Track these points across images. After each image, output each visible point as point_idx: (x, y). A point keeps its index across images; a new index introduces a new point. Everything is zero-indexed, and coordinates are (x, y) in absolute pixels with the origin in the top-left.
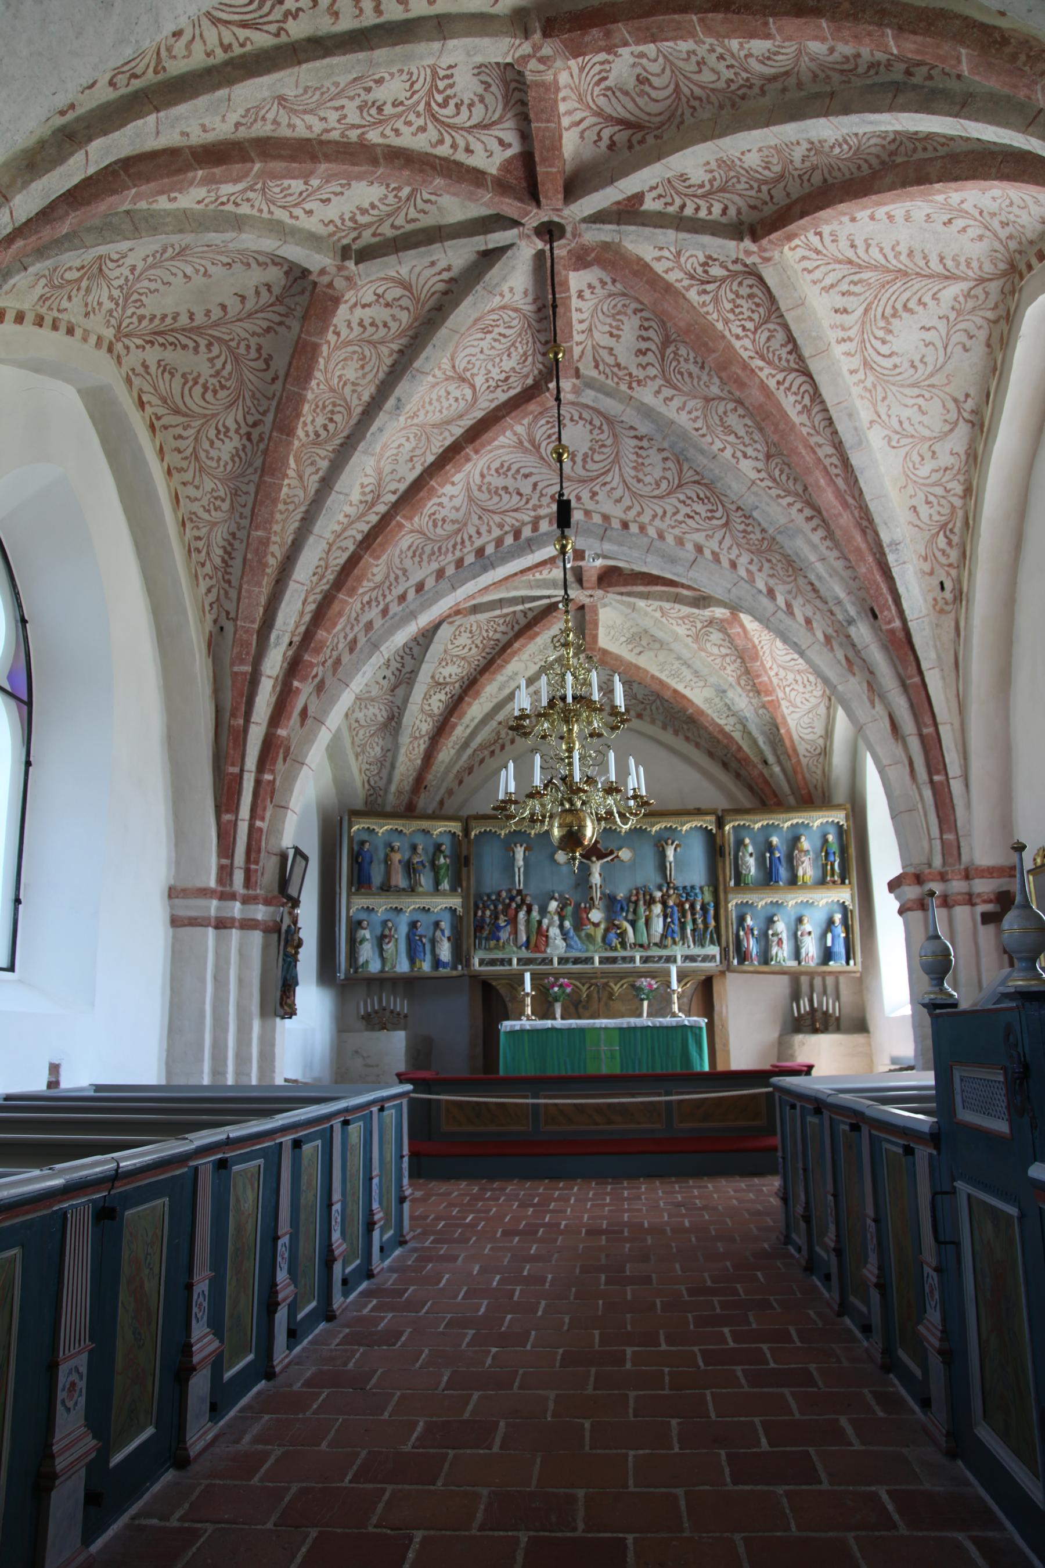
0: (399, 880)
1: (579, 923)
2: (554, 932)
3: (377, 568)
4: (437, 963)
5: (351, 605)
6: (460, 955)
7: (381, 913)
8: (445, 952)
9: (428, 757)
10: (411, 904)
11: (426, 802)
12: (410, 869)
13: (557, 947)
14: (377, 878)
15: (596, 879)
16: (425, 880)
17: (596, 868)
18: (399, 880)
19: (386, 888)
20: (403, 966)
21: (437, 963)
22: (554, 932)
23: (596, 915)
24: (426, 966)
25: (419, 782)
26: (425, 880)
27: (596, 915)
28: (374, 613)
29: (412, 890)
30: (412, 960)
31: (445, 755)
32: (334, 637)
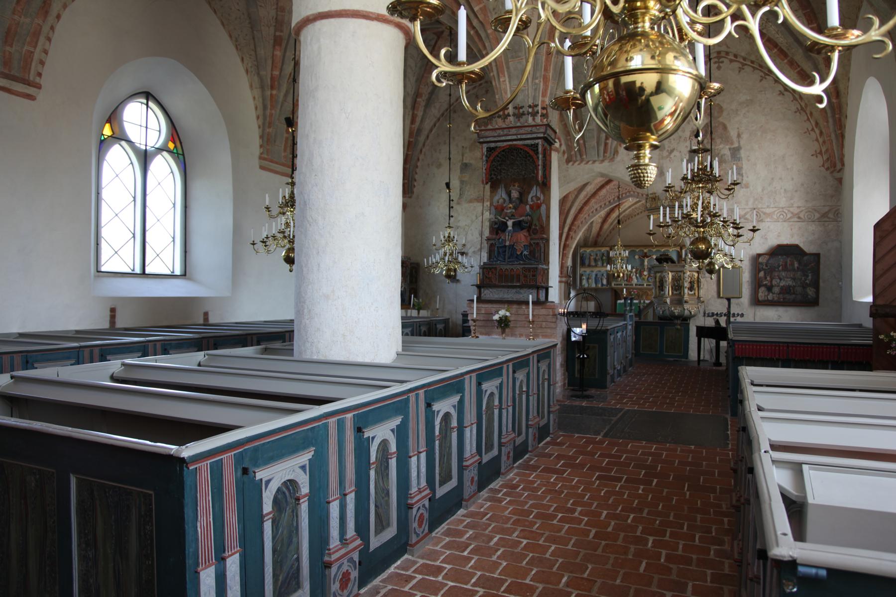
0: (593, 263)
1: (641, 275)
2: (634, 277)
3: (586, 208)
4: (602, 285)
5: (581, 216)
6: (609, 283)
7: (588, 272)
8: (605, 282)
9: (601, 228)
10: (596, 270)
11: (601, 240)
12: (595, 260)
13: (635, 281)
14: (587, 262)
15: (646, 263)
16: (600, 263)
17: (646, 260)
18: (593, 263)
19: (589, 266)
20: (594, 286)
21: (602, 285)
22: (634, 277)
23: (645, 273)
24: (600, 286)
25: (598, 235)
26: (600, 263)
27: (645, 273)
28: (586, 216)
29: (596, 266)
30: (596, 283)
31: (606, 226)
32: (577, 223)
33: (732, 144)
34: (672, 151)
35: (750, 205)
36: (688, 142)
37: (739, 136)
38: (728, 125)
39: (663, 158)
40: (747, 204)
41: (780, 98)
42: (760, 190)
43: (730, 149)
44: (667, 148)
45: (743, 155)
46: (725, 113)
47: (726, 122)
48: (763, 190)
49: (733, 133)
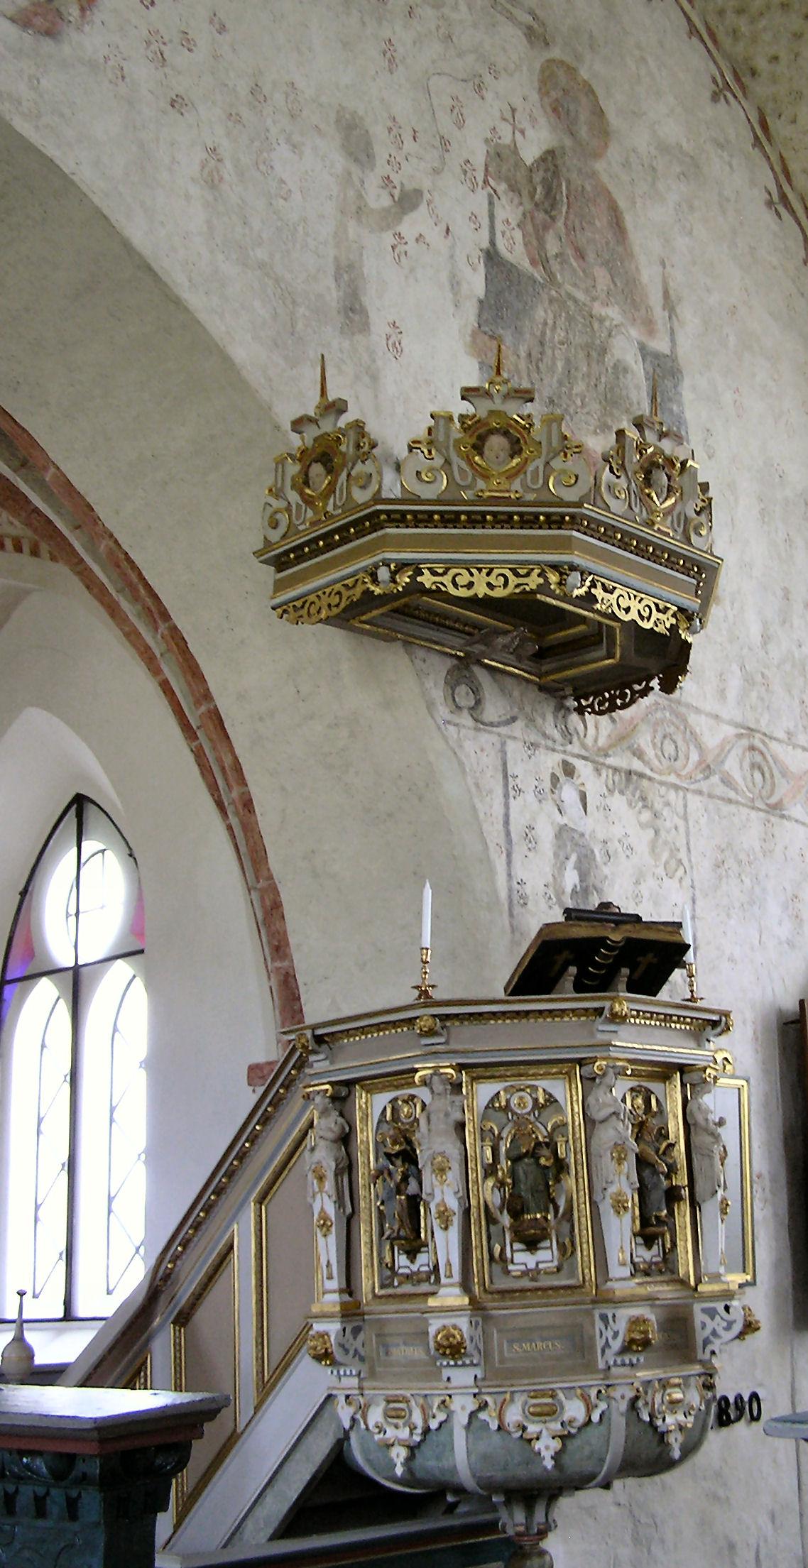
33: (649, 326)
34: (407, 201)
35: (730, 710)
36: (482, 196)
37: (670, 305)
38: (629, 220)
39: (360, 211)
40: (722, 694)
41: (768, 217)
42: (755, 631)
43: (642, 348)
44: (382, 169)
45: (689, 415)
46: (614, 152)
47: (622, 204)
48: (766, 639)
49: (649, 276)
